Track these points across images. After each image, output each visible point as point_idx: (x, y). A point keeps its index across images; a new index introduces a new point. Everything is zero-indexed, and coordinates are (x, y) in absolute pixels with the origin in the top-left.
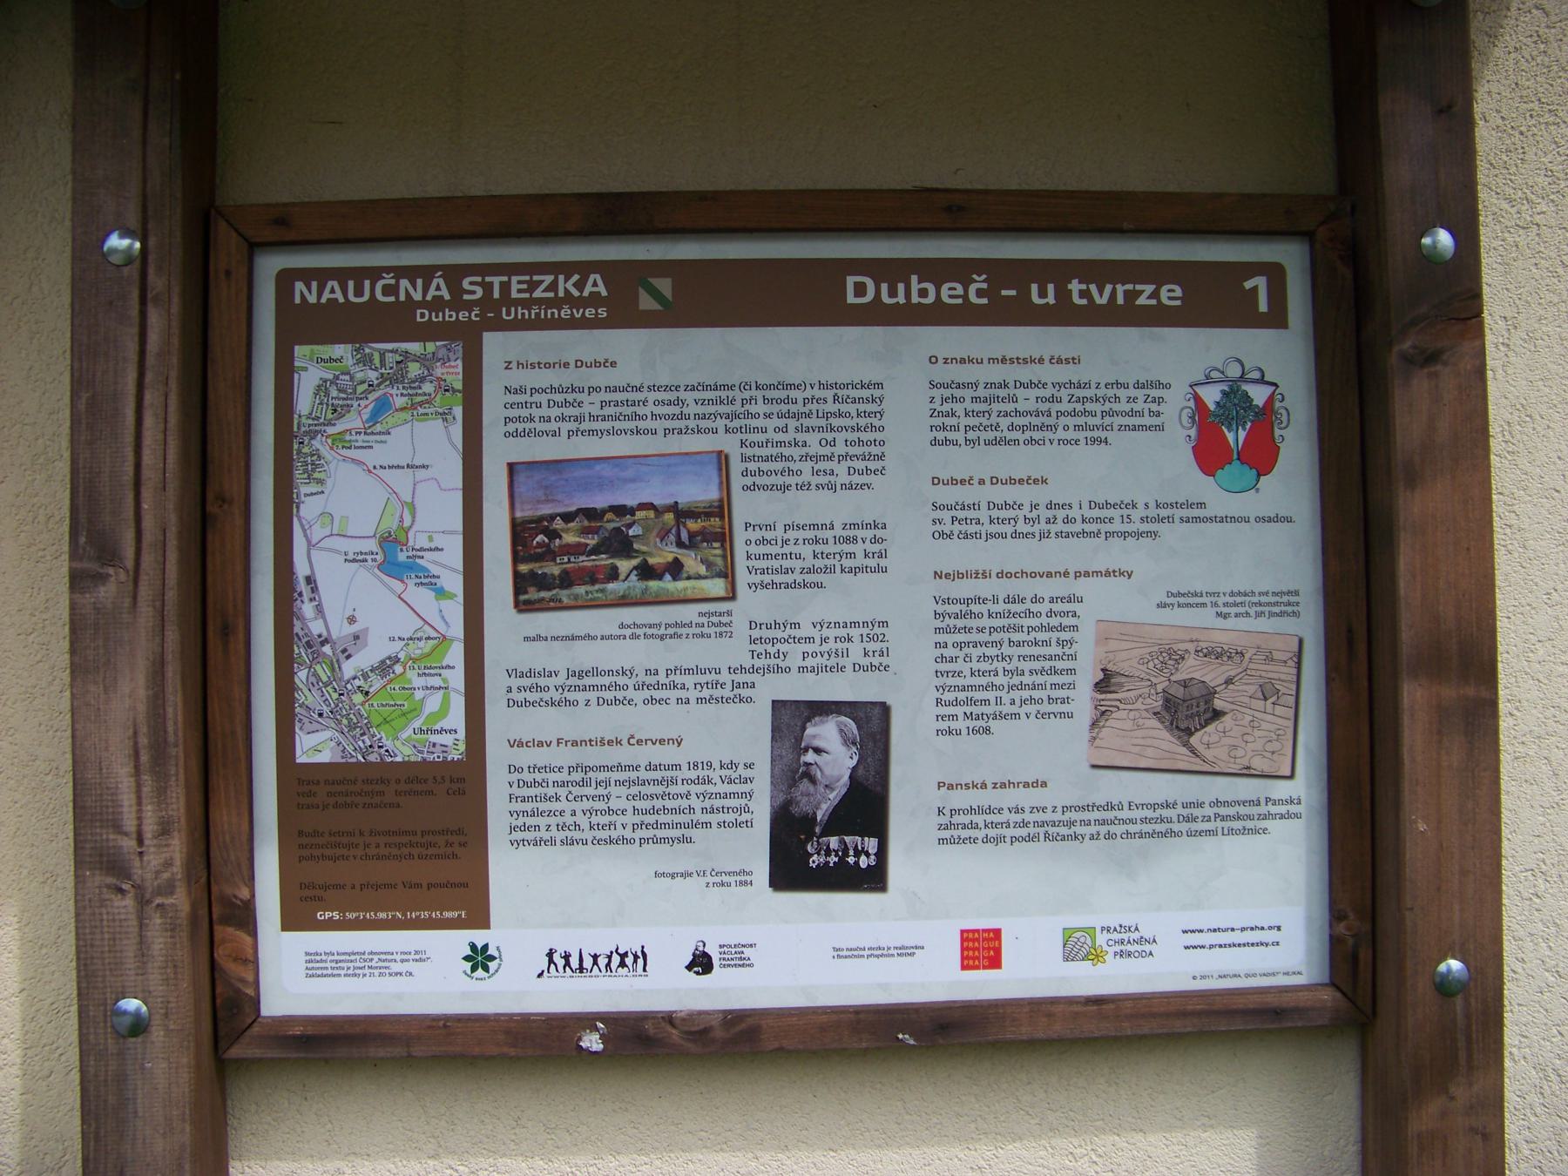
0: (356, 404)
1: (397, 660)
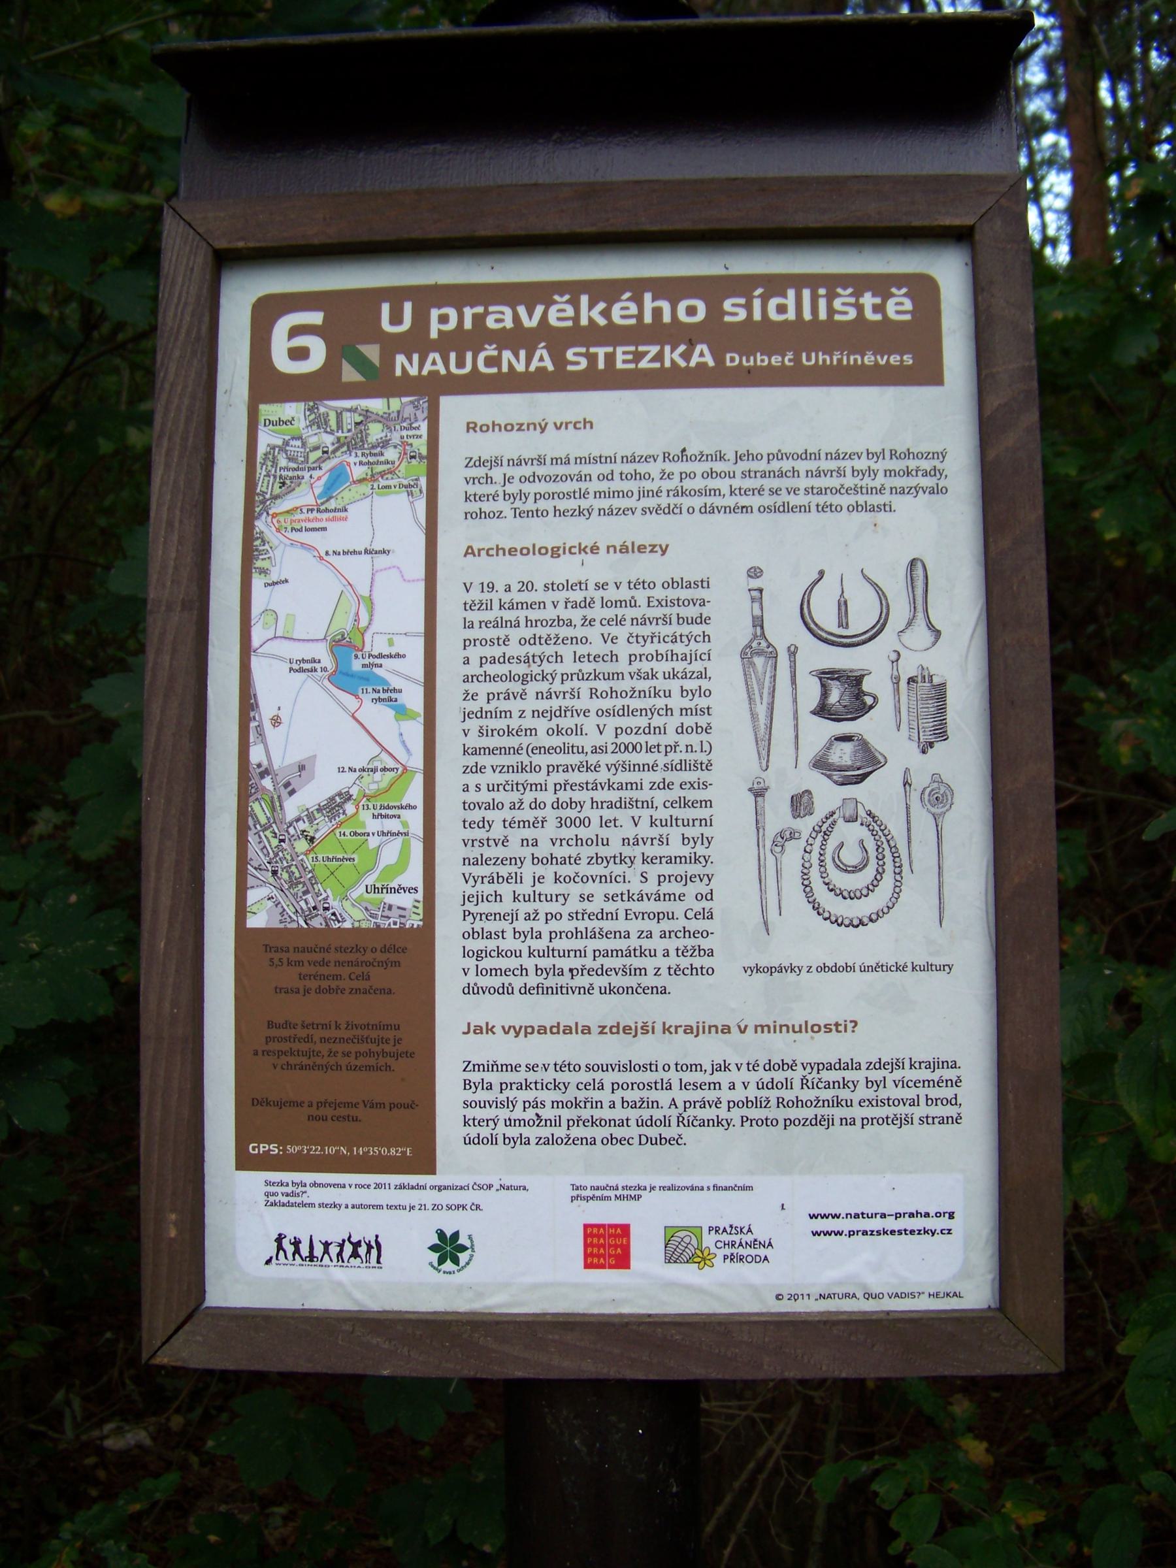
0: (307, 475)
1: (350, 797)
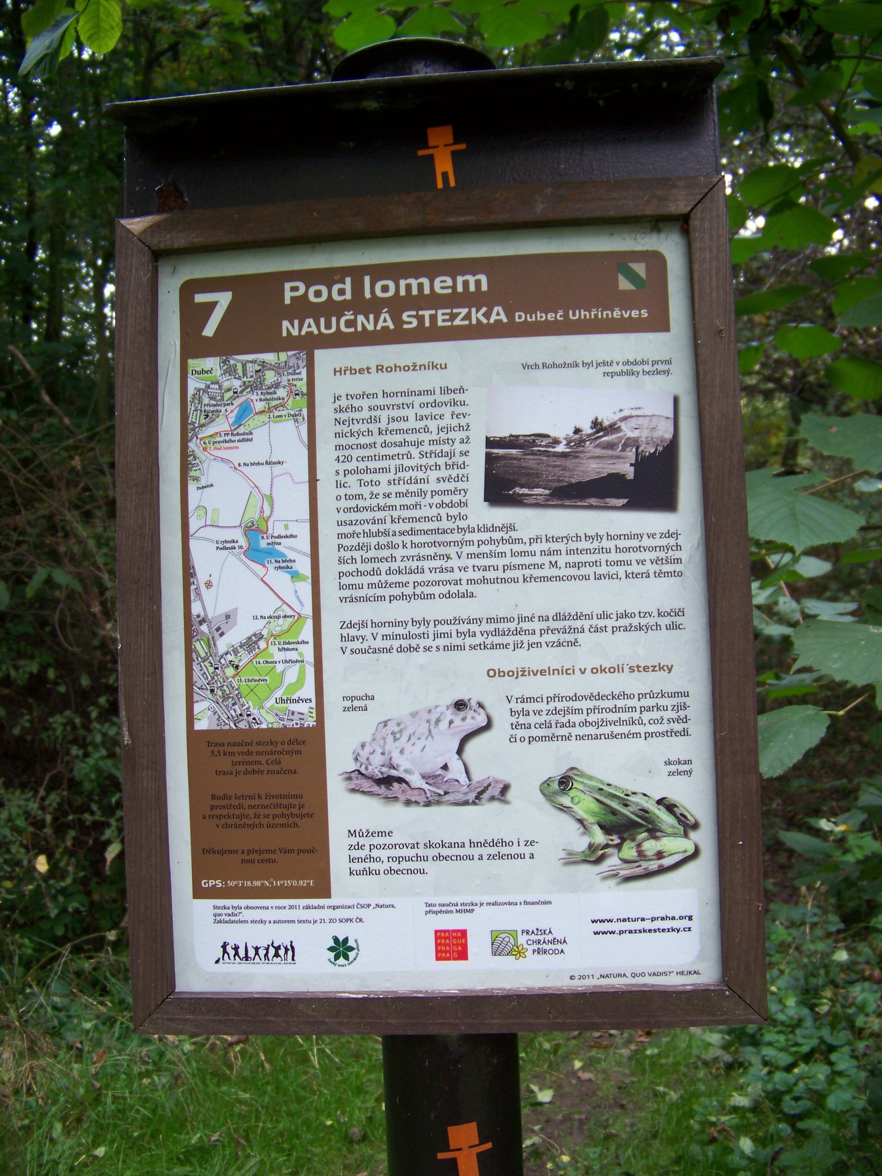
0: (223, 409)
1: (262, 637)
